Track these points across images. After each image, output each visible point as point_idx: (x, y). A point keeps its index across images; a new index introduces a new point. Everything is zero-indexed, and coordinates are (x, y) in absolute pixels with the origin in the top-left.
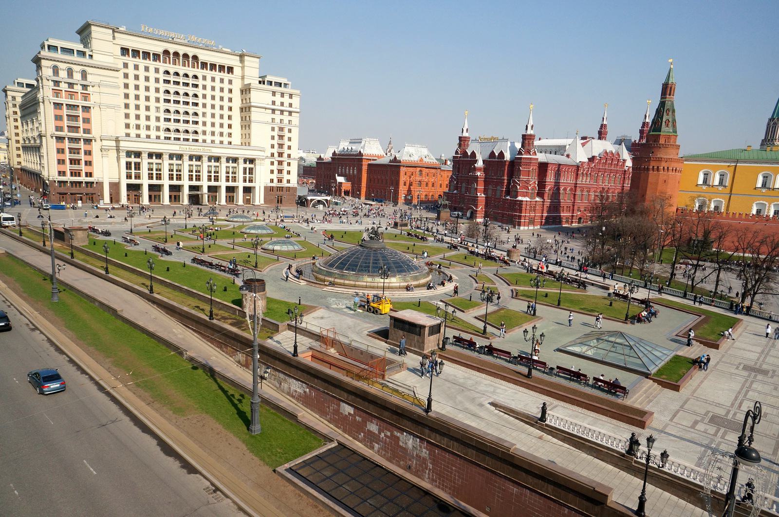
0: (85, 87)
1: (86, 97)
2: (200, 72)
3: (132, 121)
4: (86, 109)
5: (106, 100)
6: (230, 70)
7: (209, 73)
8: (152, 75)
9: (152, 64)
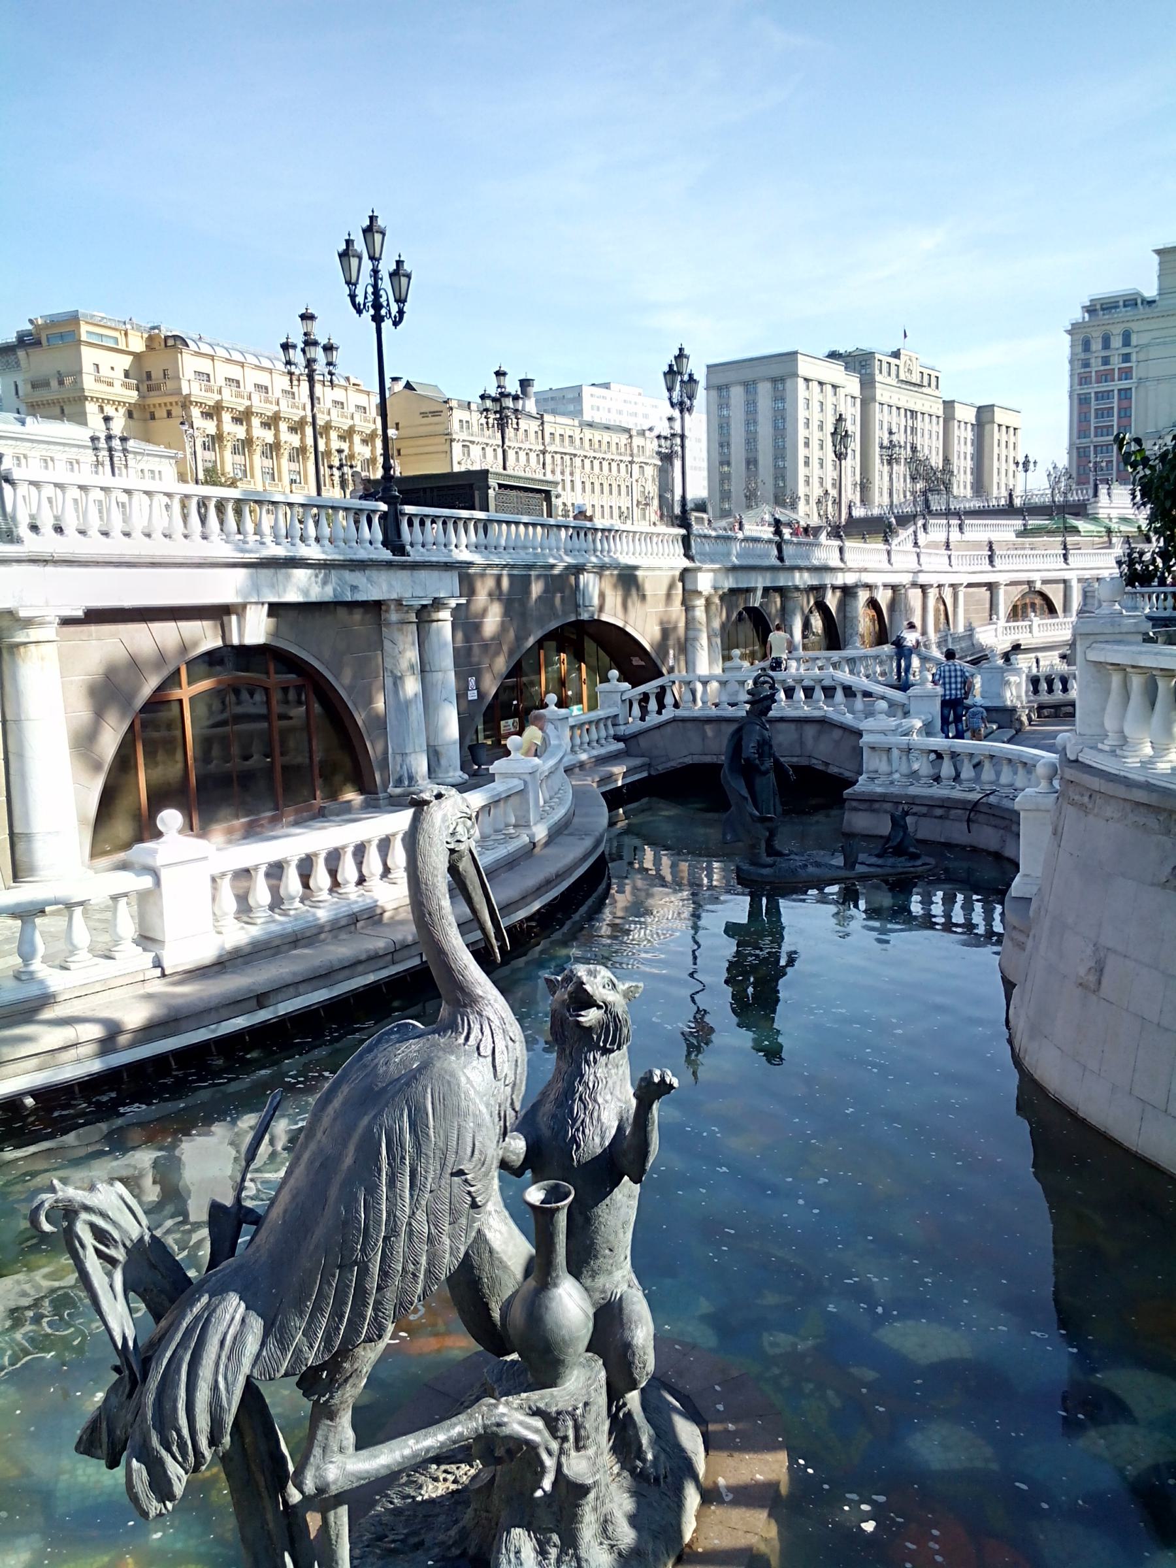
1: (1126, 374)
4: (1125, 393)
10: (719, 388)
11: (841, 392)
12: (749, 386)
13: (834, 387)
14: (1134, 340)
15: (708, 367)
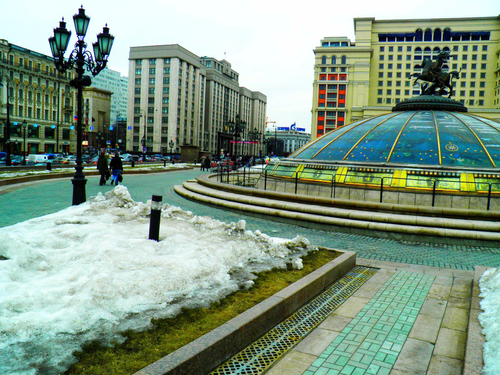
0: (343, 69)
1: (343, 77)
2: (451, 44)
3: (384, 96)
4: (343, 87)
5: (358, 77)
6: (485, 36)
7: (461, 44)
8: (404, 53)
9: (405, 44)
11: (198, 71)
12: (152, 60)
13: (195, 68)
14: (348, 61)
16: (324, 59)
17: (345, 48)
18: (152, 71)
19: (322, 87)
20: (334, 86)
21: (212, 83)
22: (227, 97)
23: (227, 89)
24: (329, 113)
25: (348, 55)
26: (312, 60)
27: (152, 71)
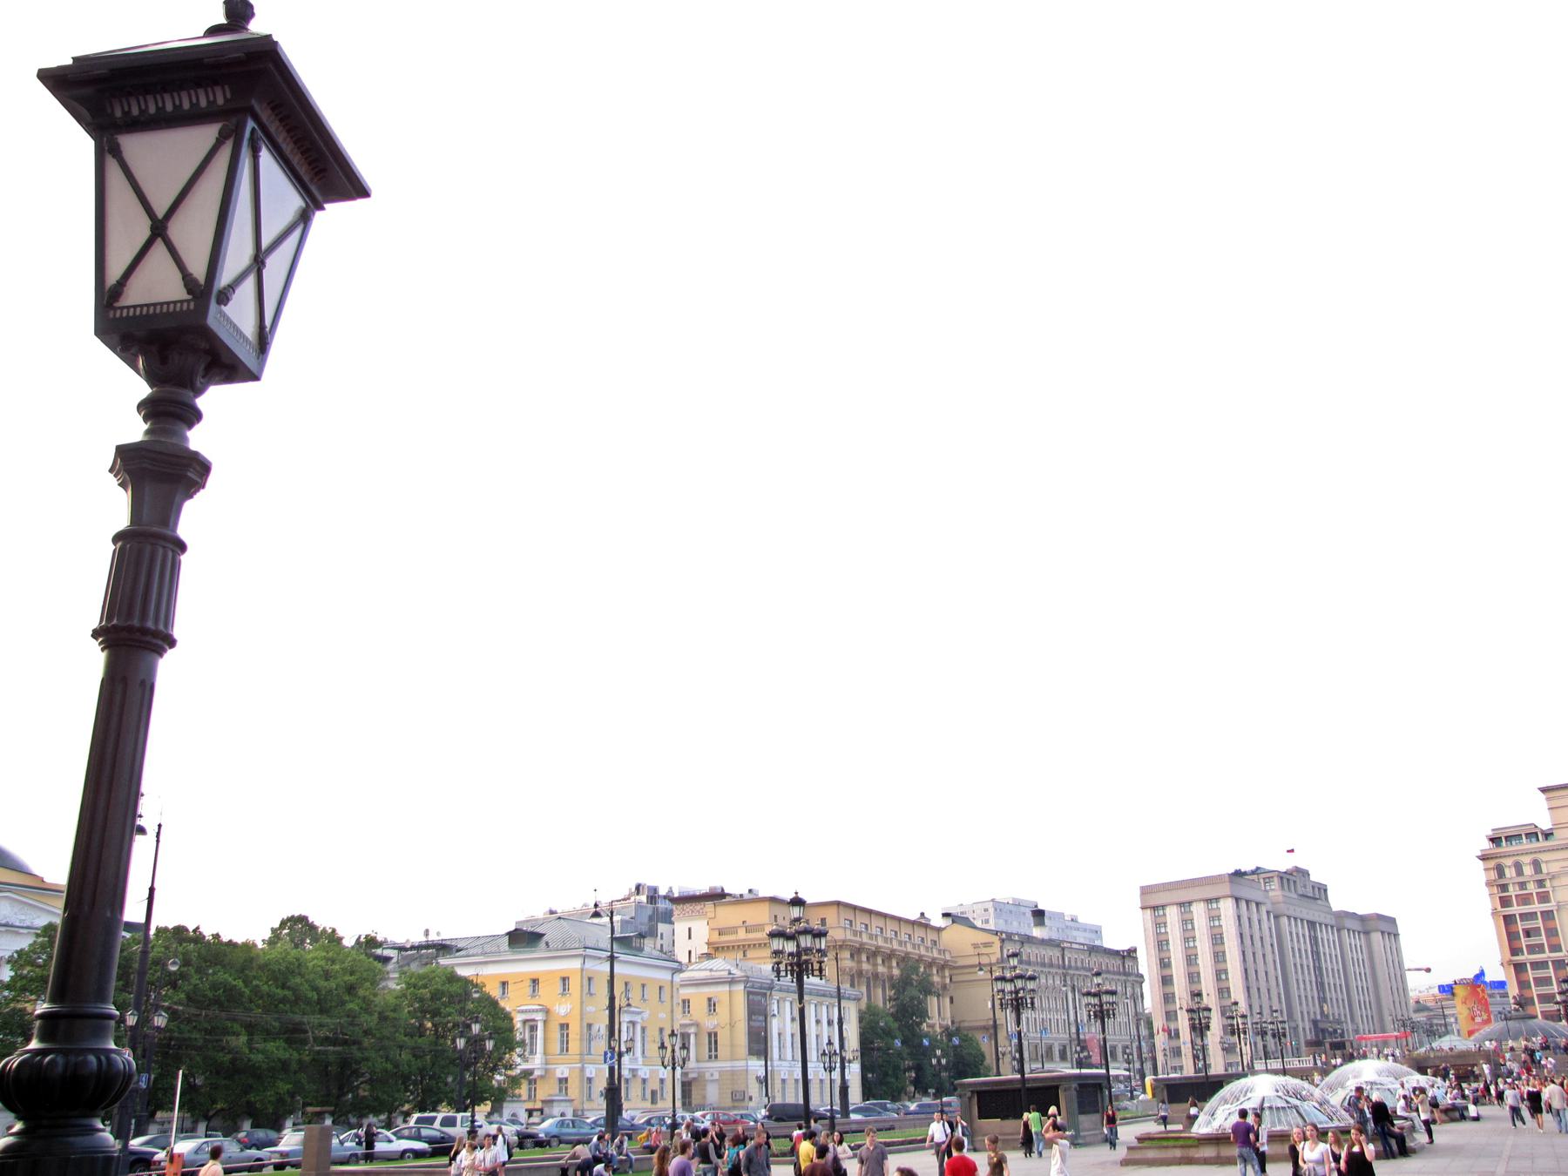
0: (1541, 883)
1: (1544, 898)
4: (1548, 915)
10: (1155, 908)
11: (1263, 909)
12: (1185, 905)
13: (1257, 904)
15: (1142, 888)
16: (1500, 870)
17: (1535, 845)
18: (1187, 922)
19: (1509, 920)
20: (1532, 916)
21: (1284, 920)
22: (1314, 940)
23: (1312, 924)
24: (1537, 965)
25: (1542, 857)
26: (1478, 874)
27: (1187, 922)
